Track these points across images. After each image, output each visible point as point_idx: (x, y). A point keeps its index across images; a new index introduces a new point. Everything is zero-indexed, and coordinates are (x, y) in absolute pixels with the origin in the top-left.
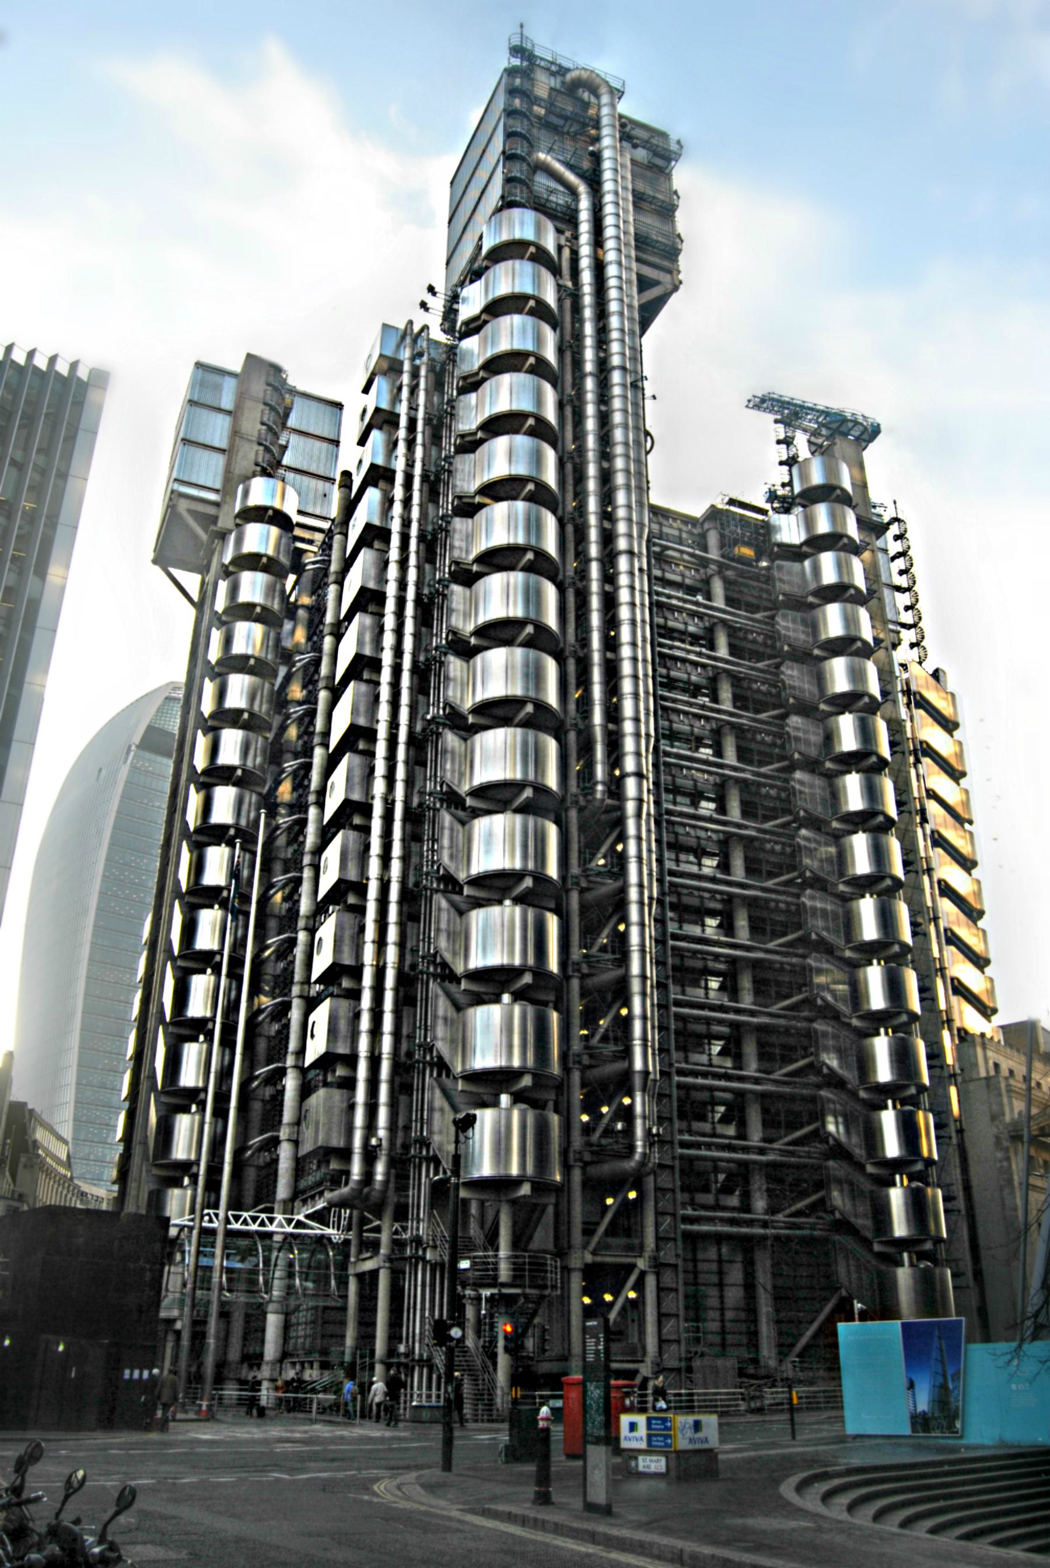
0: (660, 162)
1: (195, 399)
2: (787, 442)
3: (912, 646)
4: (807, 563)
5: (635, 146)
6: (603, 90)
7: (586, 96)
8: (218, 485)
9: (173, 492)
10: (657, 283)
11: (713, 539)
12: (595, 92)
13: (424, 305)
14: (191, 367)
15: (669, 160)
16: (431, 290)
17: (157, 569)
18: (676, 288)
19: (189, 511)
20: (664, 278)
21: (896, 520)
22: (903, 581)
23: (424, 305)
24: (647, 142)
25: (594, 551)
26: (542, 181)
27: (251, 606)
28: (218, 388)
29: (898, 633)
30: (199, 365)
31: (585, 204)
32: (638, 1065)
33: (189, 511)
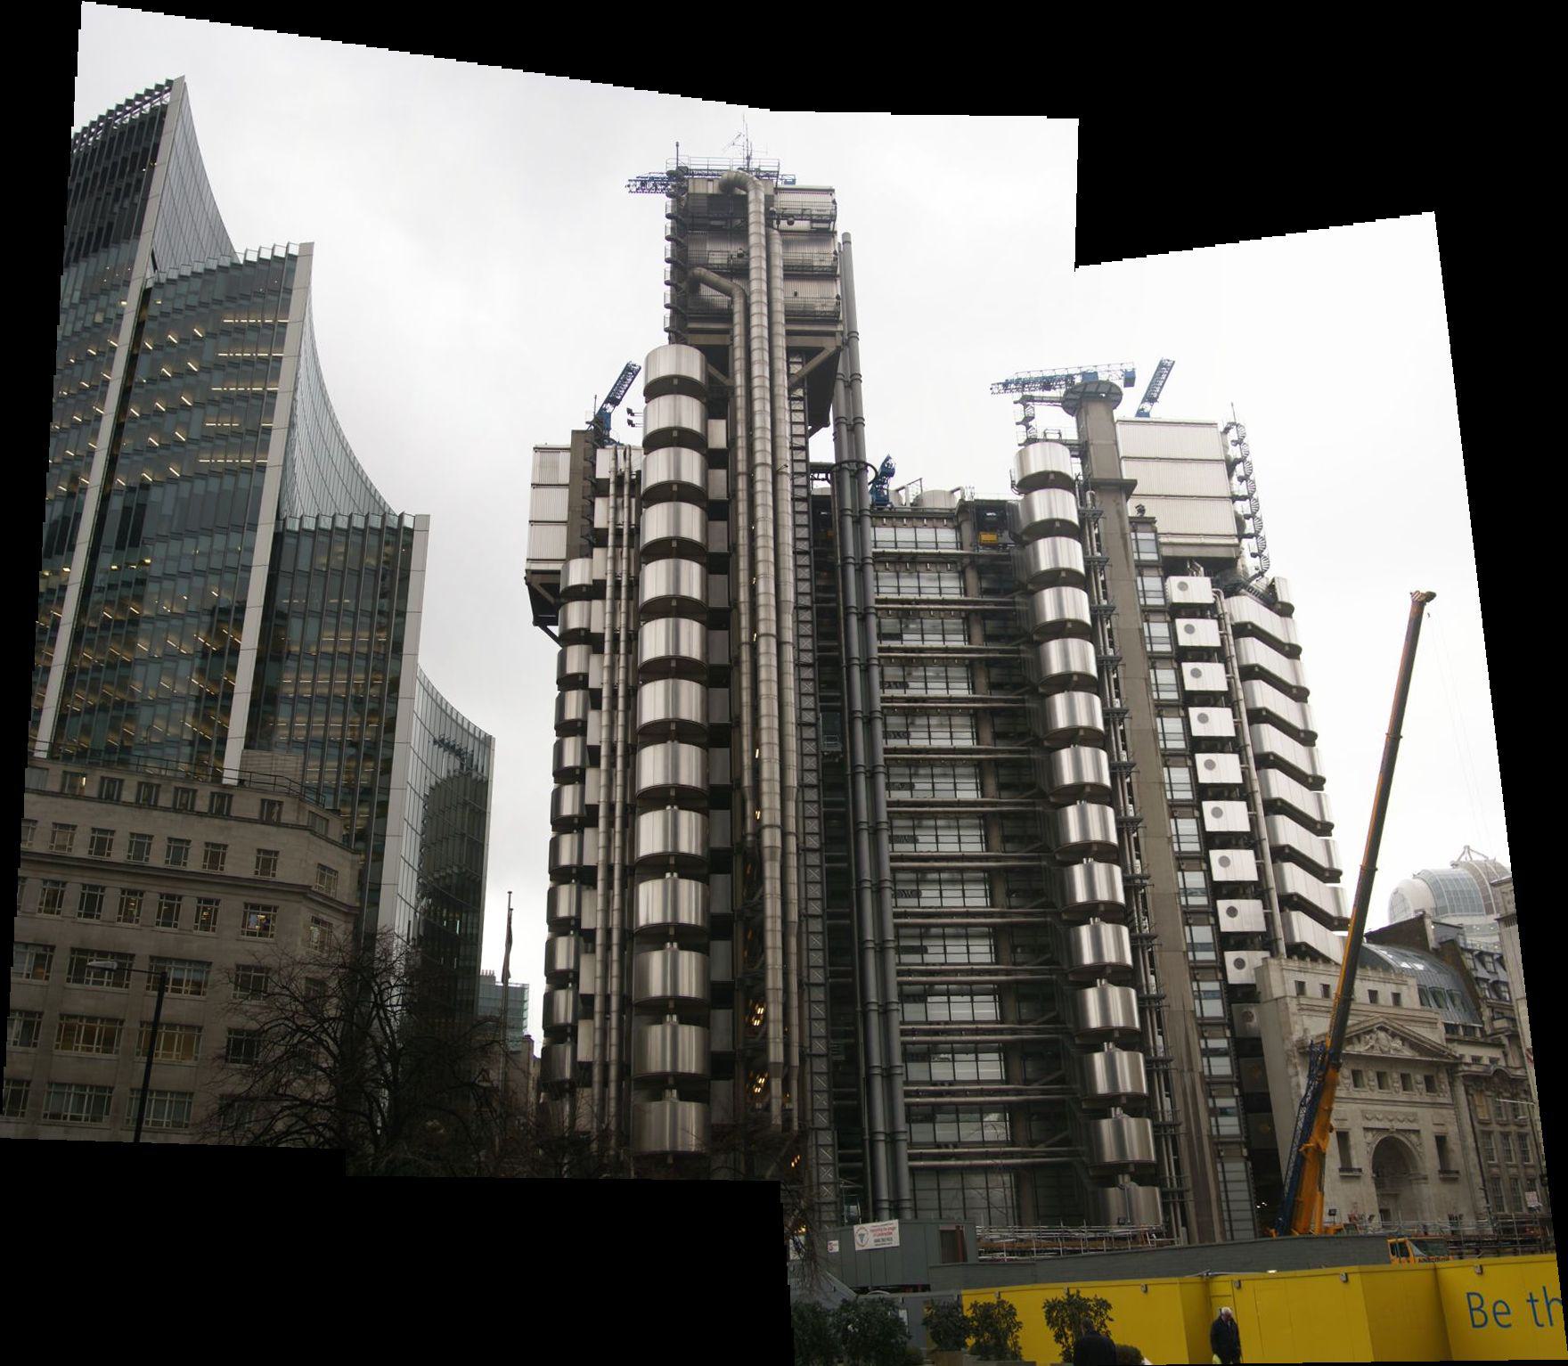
1: (537, 482)
2: (1027, 421)
3: (1254, 555)
4: (1030, 547)
5: (791, 223)
6: (750, 187)
10: (819, 350)
11: (967, 529)
12: (747, 191)
13: (630, 423)
14: (532, 452)
15: (829, 222)
16: (630, 411)
19: (541, 585)
21: (1234, 424)
22: (1241, 489)
23: (630, 423)
25: (744, 636)
26: (706, 291)
28: (555, 466)
29: (1237, 546)
30: (537, 449)
31: (738, 307)
33: (541, 585)
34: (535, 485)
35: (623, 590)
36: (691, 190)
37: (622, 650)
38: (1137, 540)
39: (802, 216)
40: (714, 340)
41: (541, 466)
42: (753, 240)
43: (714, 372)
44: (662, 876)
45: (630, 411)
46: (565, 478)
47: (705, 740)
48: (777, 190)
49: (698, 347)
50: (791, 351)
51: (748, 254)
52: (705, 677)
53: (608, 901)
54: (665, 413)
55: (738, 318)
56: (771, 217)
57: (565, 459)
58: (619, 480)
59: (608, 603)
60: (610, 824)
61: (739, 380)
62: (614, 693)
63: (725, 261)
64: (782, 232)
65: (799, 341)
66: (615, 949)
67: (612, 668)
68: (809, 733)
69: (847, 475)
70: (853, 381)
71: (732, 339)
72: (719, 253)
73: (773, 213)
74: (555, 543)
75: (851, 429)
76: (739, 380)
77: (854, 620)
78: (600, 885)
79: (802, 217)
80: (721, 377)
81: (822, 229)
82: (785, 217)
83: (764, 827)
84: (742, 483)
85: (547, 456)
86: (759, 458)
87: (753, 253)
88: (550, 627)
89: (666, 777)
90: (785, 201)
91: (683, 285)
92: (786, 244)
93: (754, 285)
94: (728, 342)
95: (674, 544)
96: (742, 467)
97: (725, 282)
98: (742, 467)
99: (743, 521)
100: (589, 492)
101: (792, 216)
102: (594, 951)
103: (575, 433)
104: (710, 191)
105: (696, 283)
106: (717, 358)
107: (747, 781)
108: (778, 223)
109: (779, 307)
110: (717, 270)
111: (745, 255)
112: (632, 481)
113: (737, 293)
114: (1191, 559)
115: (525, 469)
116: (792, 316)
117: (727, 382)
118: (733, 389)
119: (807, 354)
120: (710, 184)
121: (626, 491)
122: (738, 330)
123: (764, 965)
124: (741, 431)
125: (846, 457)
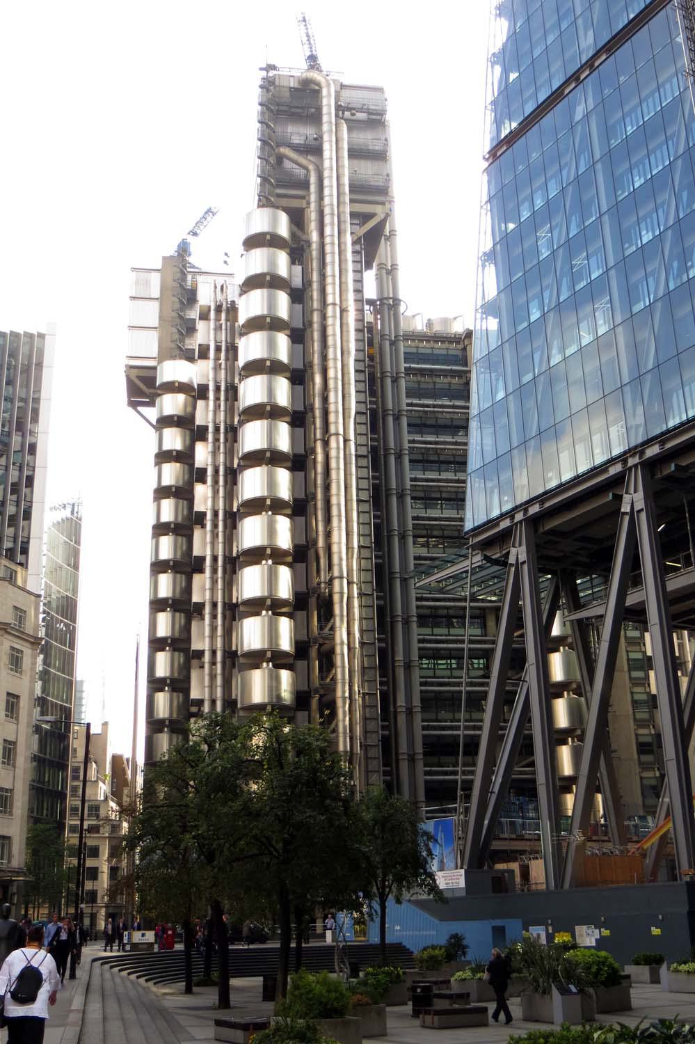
0: (379, 117)
1: (134, 295)
7: (317, 88)
8: (155, 355)
9: (126, 366)
13: (225, 262)
16: (226, 254)
17: (131, 409)
18: (387, 215)
19: (137, 377)
20: (379, 210)
23: (225, 262)
24: (362, 108)
26: (288, 165)
27: (169, 452)
30: (134, 269)
32: (341, 748)
33: (137, 377)
34: (133, 298)
35: (222, 393)
36: (277, 83)
37: (222, 440)
39: (361, 110)
40: (295, 203)
41: (137, 283)
42: (325, 127)
43: (295, 229)
44: (258, 614)
45: (226, 254)
46: (156, 292)
47: (289, 511)
48: (343, 86)
49: (286, 210)
50: (353, 215)
51: (322, 138)
52: (289, 464)
53: (213, 629)
54: (257, 261)
55: (313, 188)
56: (338, 108)
57: (155, 280)
58: (219, 309)
59: (211, 403)
60: (214, 571)
61: (315, 237)
62: (216, 471)
63: (302, 142)
64: (346, 120)
65: (360, 208)
66: (219, 666)
67: (215, 453)
68: (365, 507)
69: (386, 308)
70: (392, 233)
71: (309, 203)
72: (298, 133)
73: (341, 106)
74: (148, 346)
75: (389, 273)
76: (315, 237)
77: (390, 420)
78: (207, 617)
79: (361, 110)
80: (299, 233)
81: (375, 120)
82: (349, 109)
83: (335, 578)
84: (316, 317)
85: (143, 275)
86: (330, 299)
87: (326, 137)
88: (140, 409)
89: (263, 540)
90: (346, 94)
91: (272, 160)
92: (350, 129)
93: (326, 164)
95: (268, 363)
96: (316, 305)
98: (316, 305)
99: (317, 346)
100: (177, 306)
101: (354, 109)
102: (202, 667)
103: (164, 258)
104: (292, 85)
105: (280, 159)
106: (297, 219)
107: (321, 543)
108: (343, 113)
109: (346, 181)
110: (297, 148)
111: (319, 139)
112: (228, 308)
113: (311, 167)
116: (354, 188)
117: (304, 237)
118: (309, 243)
119: (366, 217)
120: (292, 78)
121: (223, 315)
122: (313, 198)
123: (334, 679)
124: (315, 277)
125: (386, 296)
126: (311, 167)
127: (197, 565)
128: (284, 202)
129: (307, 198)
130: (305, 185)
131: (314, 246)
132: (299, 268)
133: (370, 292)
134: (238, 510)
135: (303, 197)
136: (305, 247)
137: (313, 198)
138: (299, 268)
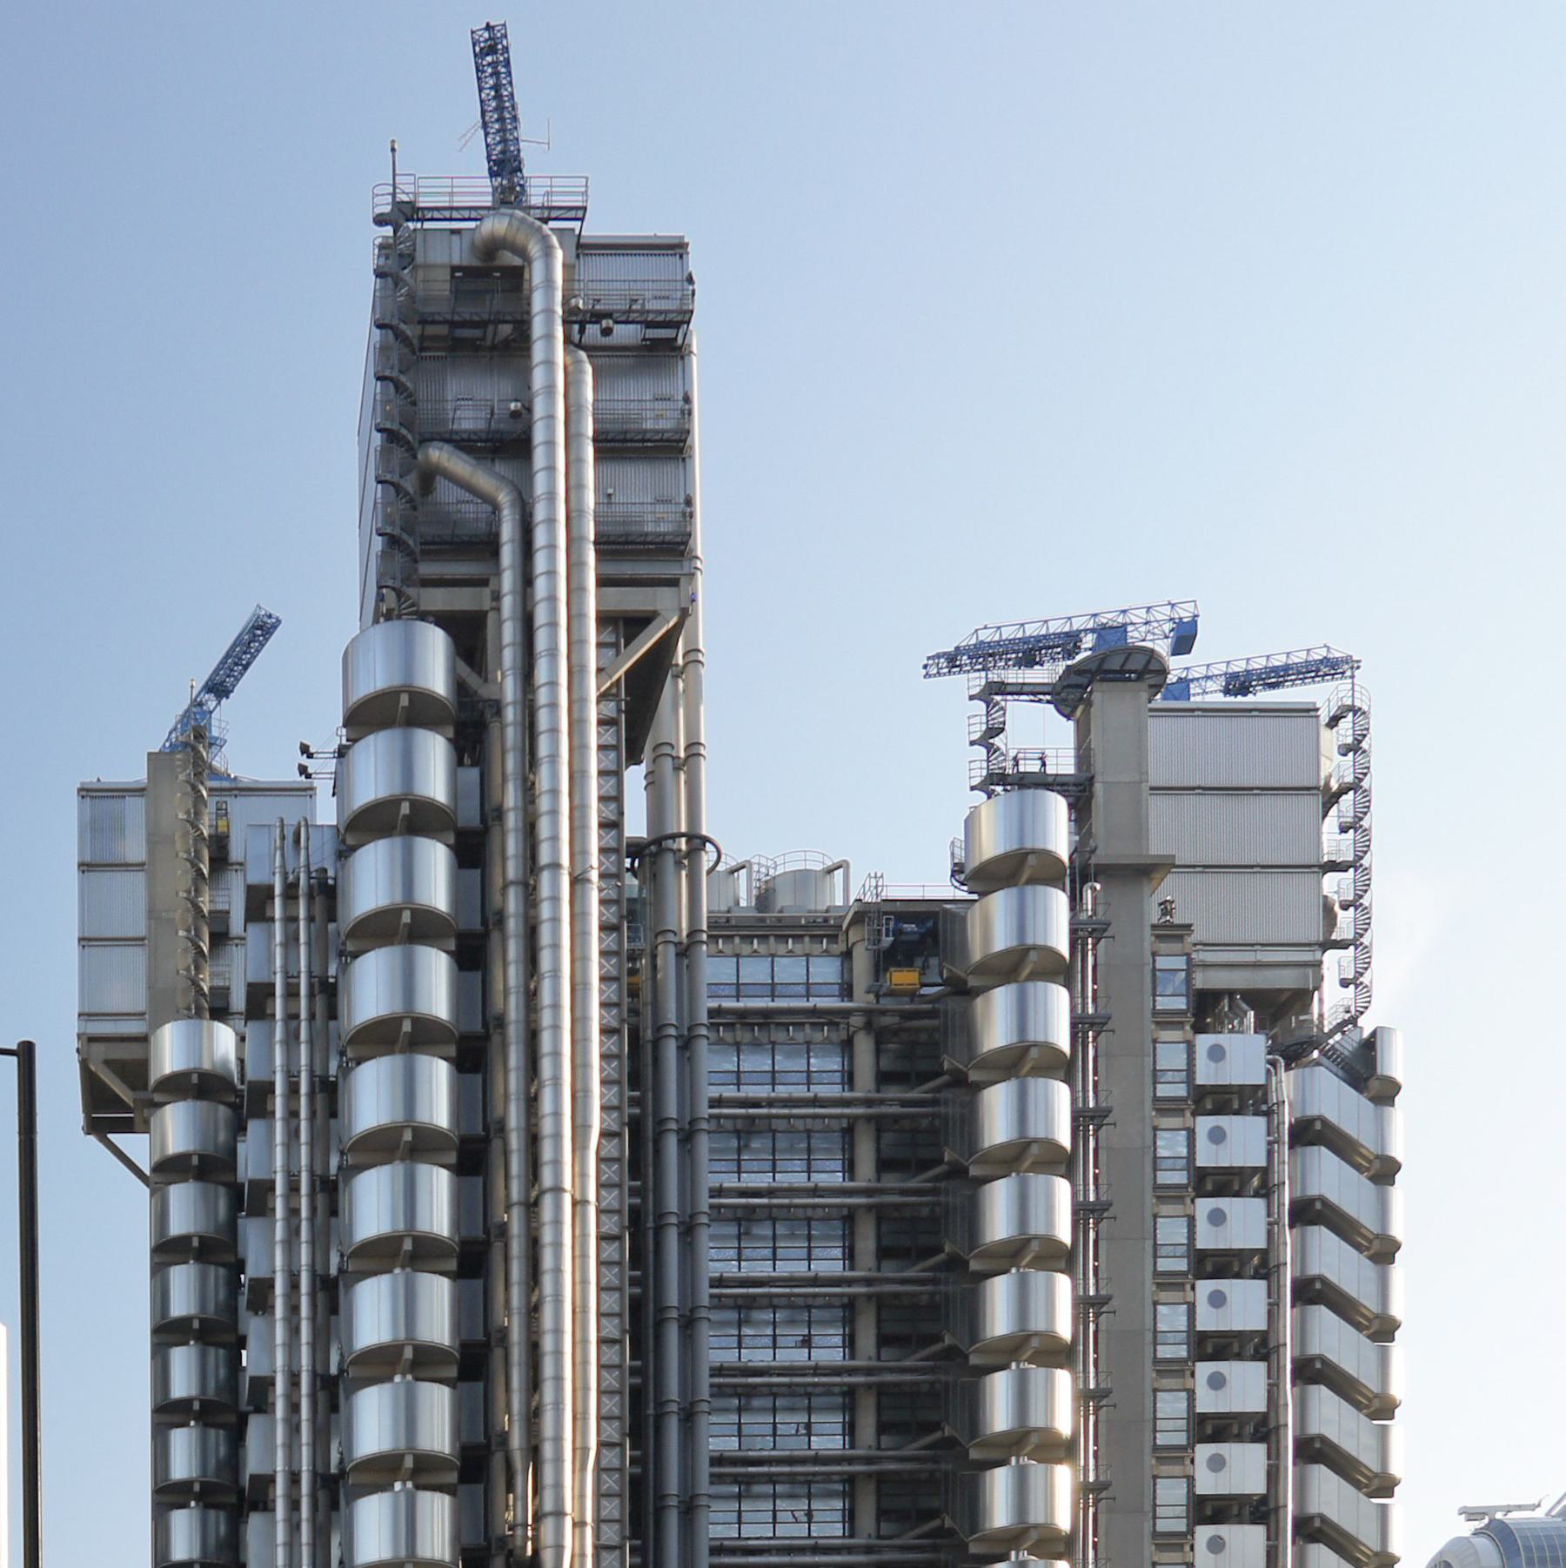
38: (1154, 969)
55: (508, 555)
71: (497, 597)
94: (487, 604)
97: (483, 480)
113: (504, 498)
114: (1231, 993)
115: (67, 817)
117: (485, 692)
126: (504, 498)
127: (257, 1497)
128: (437, 599)
129: (492, 581)
130: (489, 547)
131: (510, 714)
132: (473, 774)
133: (636, 826)
134: (341, 1371)
135: (482, 582)
136: (488, 715)
137: (508, 581)
138: (473, 774)
